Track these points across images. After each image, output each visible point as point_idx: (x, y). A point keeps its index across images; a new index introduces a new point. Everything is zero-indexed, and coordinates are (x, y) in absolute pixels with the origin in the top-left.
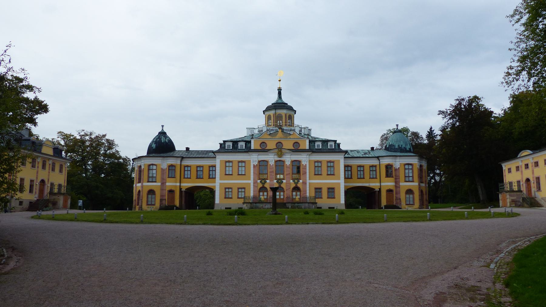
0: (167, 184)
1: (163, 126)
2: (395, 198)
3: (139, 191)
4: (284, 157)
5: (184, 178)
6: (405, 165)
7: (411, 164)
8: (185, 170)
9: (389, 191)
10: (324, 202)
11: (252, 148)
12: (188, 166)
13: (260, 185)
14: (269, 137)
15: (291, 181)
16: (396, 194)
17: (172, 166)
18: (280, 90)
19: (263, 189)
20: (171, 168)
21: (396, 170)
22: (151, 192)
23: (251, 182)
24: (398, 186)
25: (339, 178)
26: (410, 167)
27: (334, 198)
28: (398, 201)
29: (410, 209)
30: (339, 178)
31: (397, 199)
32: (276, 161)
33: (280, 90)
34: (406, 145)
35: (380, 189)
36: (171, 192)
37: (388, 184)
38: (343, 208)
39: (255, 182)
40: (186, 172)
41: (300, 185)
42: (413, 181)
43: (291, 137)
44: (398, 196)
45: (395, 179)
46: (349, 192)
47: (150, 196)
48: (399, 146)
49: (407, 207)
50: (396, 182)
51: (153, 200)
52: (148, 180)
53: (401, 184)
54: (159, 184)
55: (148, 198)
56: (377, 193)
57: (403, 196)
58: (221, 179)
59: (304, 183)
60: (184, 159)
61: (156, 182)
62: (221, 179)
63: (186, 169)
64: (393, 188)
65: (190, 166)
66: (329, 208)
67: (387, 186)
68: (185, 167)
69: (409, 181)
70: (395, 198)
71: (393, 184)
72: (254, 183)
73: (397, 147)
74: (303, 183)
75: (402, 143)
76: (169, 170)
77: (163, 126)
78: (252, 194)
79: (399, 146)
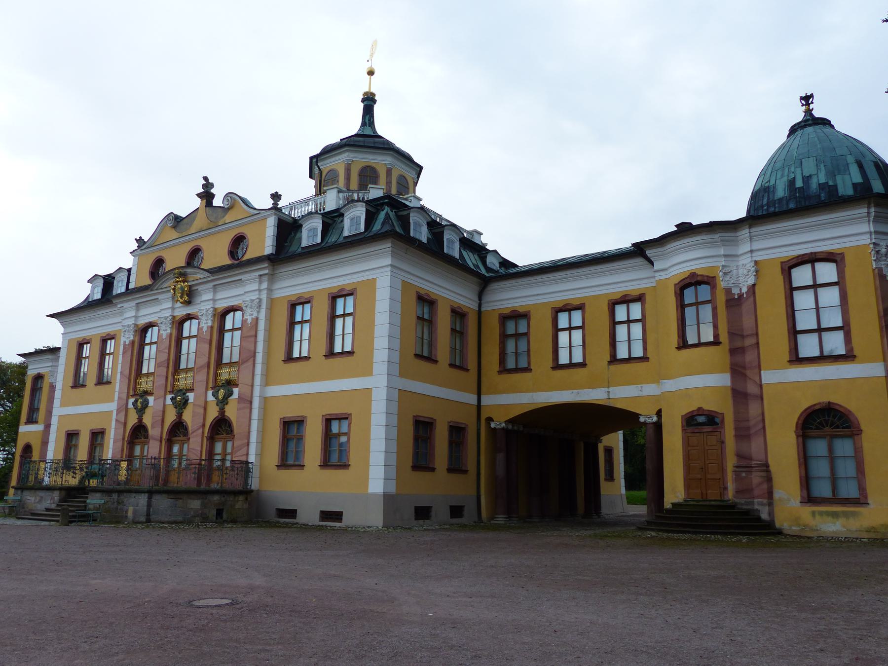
2: (731, 462)
4: (198, 300)
6: (789, 267)
7: (829, 257)
9: (701, 423)
10: (307, 487)
13: (133, 420)
14: (174, 234)
15: (210, 398)
16: (743, 434)
18: (369, 101)
19: (139, 432)
21: (734, 302)
23: (112, 406)
24: (752, 389)
25: (367, 371)
26: (827, 272)
27: (346, 466)
28: (756, 478)
29: (832, 525)
30: (367, 371)
31: (745, 463)
32: (179, 324)
33: (369, 101)
34: (832, 174)
35: (659, 413)
37: (701, 382)
38: (375, 518)
39: (123, 409)
41: (231, 412)
42: (848, 357)
43: (228, 218)
44: (755, 448)
45: (733, 351)
46: (420, 437)
48: (792, 182)
49: (806, 513)
50: (738, 371)
53: (768, 377)
56: (651, 431)
57: (781, 446)
58: (63, 404)
59: (246, 401)
64: (724, 407)
66: (327, 515)
67: (686, 393)
69: (823, 358)
70: (731, 462)
71: (723, 380)
72: (119, 411)
73: (781, 192)
74: (241, 399)
75: (809, 167)
78: (110, 457)
79: (792, 182)
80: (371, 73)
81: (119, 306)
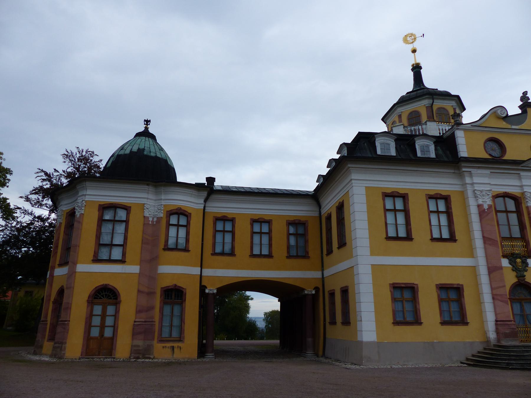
0: (164, 269)
1: (147, 122)
3: (61, 292)
5: (214, 254)
8: (216, 231)
11: (463, 151)
12: (224, 219)
17: (180, 212)
18: (417, 69)
20: (173, 220)
22: (105, 294)
33: (417, 69)
36: (174, 294)
40: (219, 237)
47: (98, 309)
51: (109, 321)
52: (96, 254)
54: (135, 269)
55: (90, 316)
58: (373, 253)
60: (214, 196)
61: (122, 261)
62: (373, 253)
63: (220, 226)
65: (232, 220)
68: (217, 219)
76: (169, 225)
77: (147, 122)
80: (414, 51)
81: (464, 169)
